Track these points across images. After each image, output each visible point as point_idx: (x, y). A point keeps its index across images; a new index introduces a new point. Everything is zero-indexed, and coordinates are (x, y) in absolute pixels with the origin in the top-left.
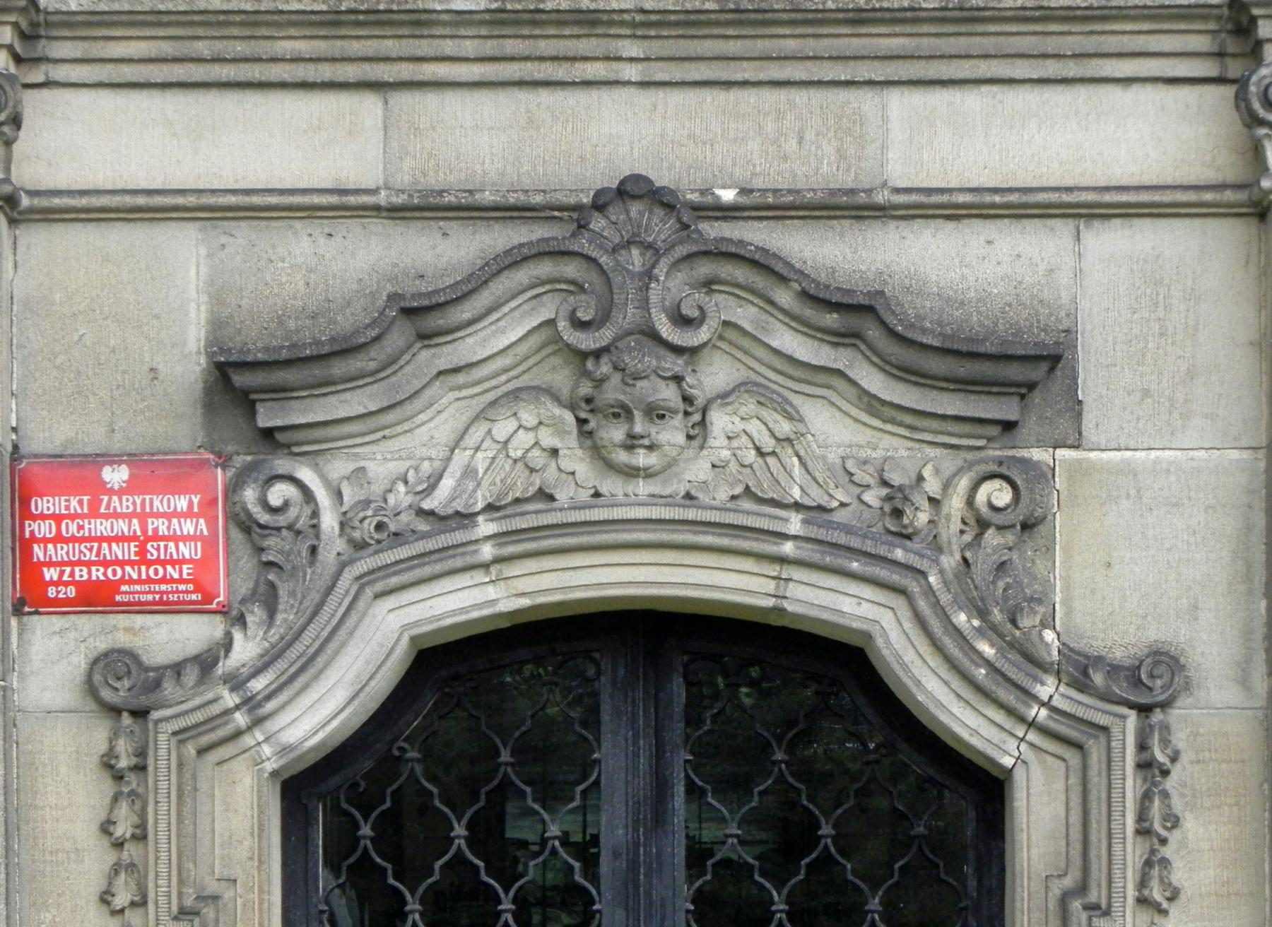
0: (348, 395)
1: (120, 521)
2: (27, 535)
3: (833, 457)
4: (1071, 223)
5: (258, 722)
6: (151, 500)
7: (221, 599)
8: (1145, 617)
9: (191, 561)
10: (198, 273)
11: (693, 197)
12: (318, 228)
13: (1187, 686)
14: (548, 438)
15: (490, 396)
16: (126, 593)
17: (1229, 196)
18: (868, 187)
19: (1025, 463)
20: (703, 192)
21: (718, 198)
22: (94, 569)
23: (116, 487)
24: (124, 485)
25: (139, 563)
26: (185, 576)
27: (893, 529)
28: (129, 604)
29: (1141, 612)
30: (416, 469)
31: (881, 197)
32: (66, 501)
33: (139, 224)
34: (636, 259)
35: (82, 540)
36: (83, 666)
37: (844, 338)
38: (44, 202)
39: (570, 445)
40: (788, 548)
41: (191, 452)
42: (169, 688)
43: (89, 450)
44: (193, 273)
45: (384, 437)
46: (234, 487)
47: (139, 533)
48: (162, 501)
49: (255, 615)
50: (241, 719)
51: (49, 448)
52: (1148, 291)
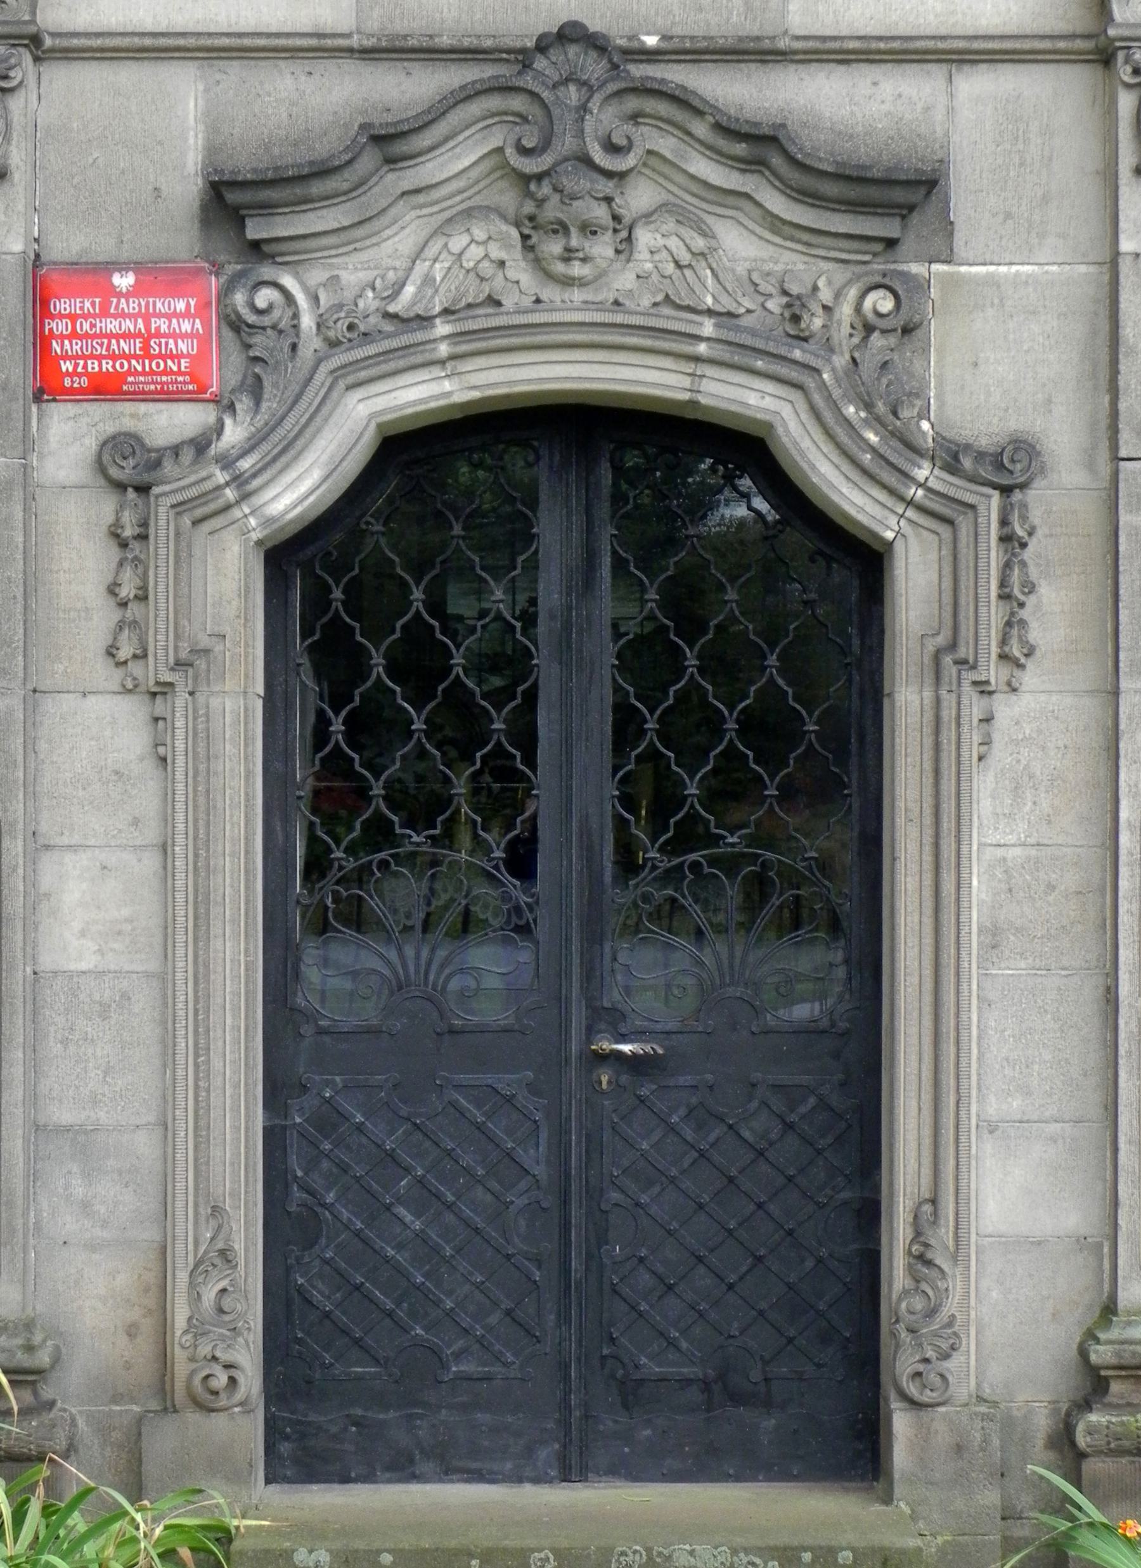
0: (324, 212)
1: (128, 321)
2: (47, 332)
3: (741, 269)
4: (945, 67)
5: (245, 497)
7: (214, 389)
8: (1006, 410)
9: (188, 356)
10: (196, 105)
11: (622, 42)
12: (300, 67)
13: (1042, 470)
14: (496, 252)
15: (447, 214)
16: (132, 383)
17: (1080, 44)
18: (771, 34)
19: (905, 276)
20: (631, 38)
21: (643, 43)
22: (104, 362)
23: (124, 290)
25: (143, 357)
26: (183, 369)
27: (792, 332)
28: (134, 393)
29: (1003, 405)
30: (383, 277)
31: (783, 44)
33: (146, 63)
34: (573, 94)
35: (94, 336)
36: (94, 447)
37: (752, 164)
38: (65, 43)
39: (515, 258)
40: (702, 348)
41: (189, 261)
42: (168, 466)
43: (100, 259)
44: (192, 104)
45: (355, 249)
46: (227, 291)
47: (143, 331)
48: (163, 304)
49: (244, 404)
50: (230, 494)
51: (66, 257)
52: (1010, 127)
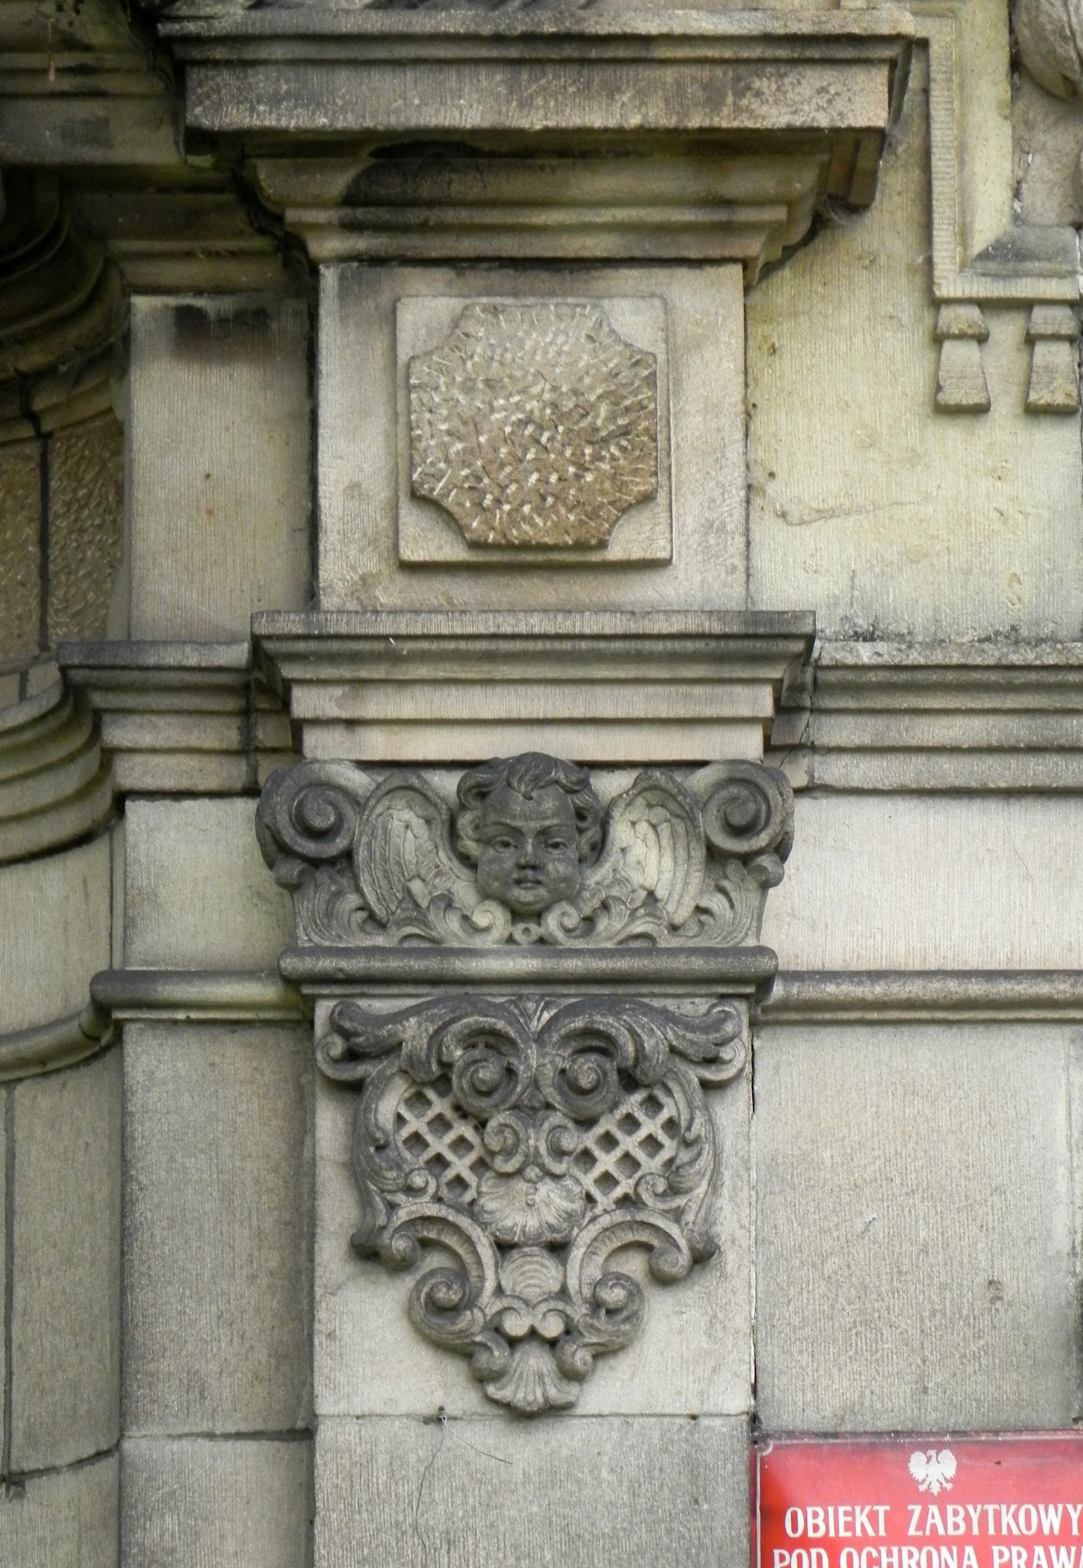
6: (997, 1515)
23: (935, 1490)
24: (949, 1486)
32: (846, 1514)
33: (967, 1030)
41: (1064, 1429)
43: (882, 1425)
